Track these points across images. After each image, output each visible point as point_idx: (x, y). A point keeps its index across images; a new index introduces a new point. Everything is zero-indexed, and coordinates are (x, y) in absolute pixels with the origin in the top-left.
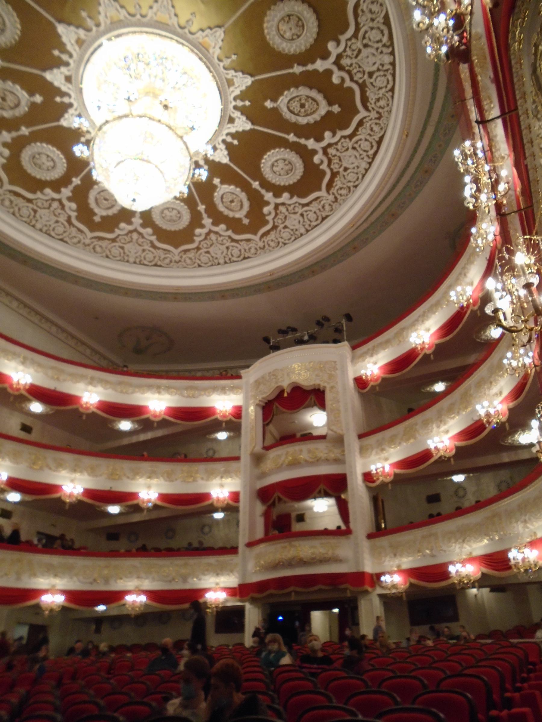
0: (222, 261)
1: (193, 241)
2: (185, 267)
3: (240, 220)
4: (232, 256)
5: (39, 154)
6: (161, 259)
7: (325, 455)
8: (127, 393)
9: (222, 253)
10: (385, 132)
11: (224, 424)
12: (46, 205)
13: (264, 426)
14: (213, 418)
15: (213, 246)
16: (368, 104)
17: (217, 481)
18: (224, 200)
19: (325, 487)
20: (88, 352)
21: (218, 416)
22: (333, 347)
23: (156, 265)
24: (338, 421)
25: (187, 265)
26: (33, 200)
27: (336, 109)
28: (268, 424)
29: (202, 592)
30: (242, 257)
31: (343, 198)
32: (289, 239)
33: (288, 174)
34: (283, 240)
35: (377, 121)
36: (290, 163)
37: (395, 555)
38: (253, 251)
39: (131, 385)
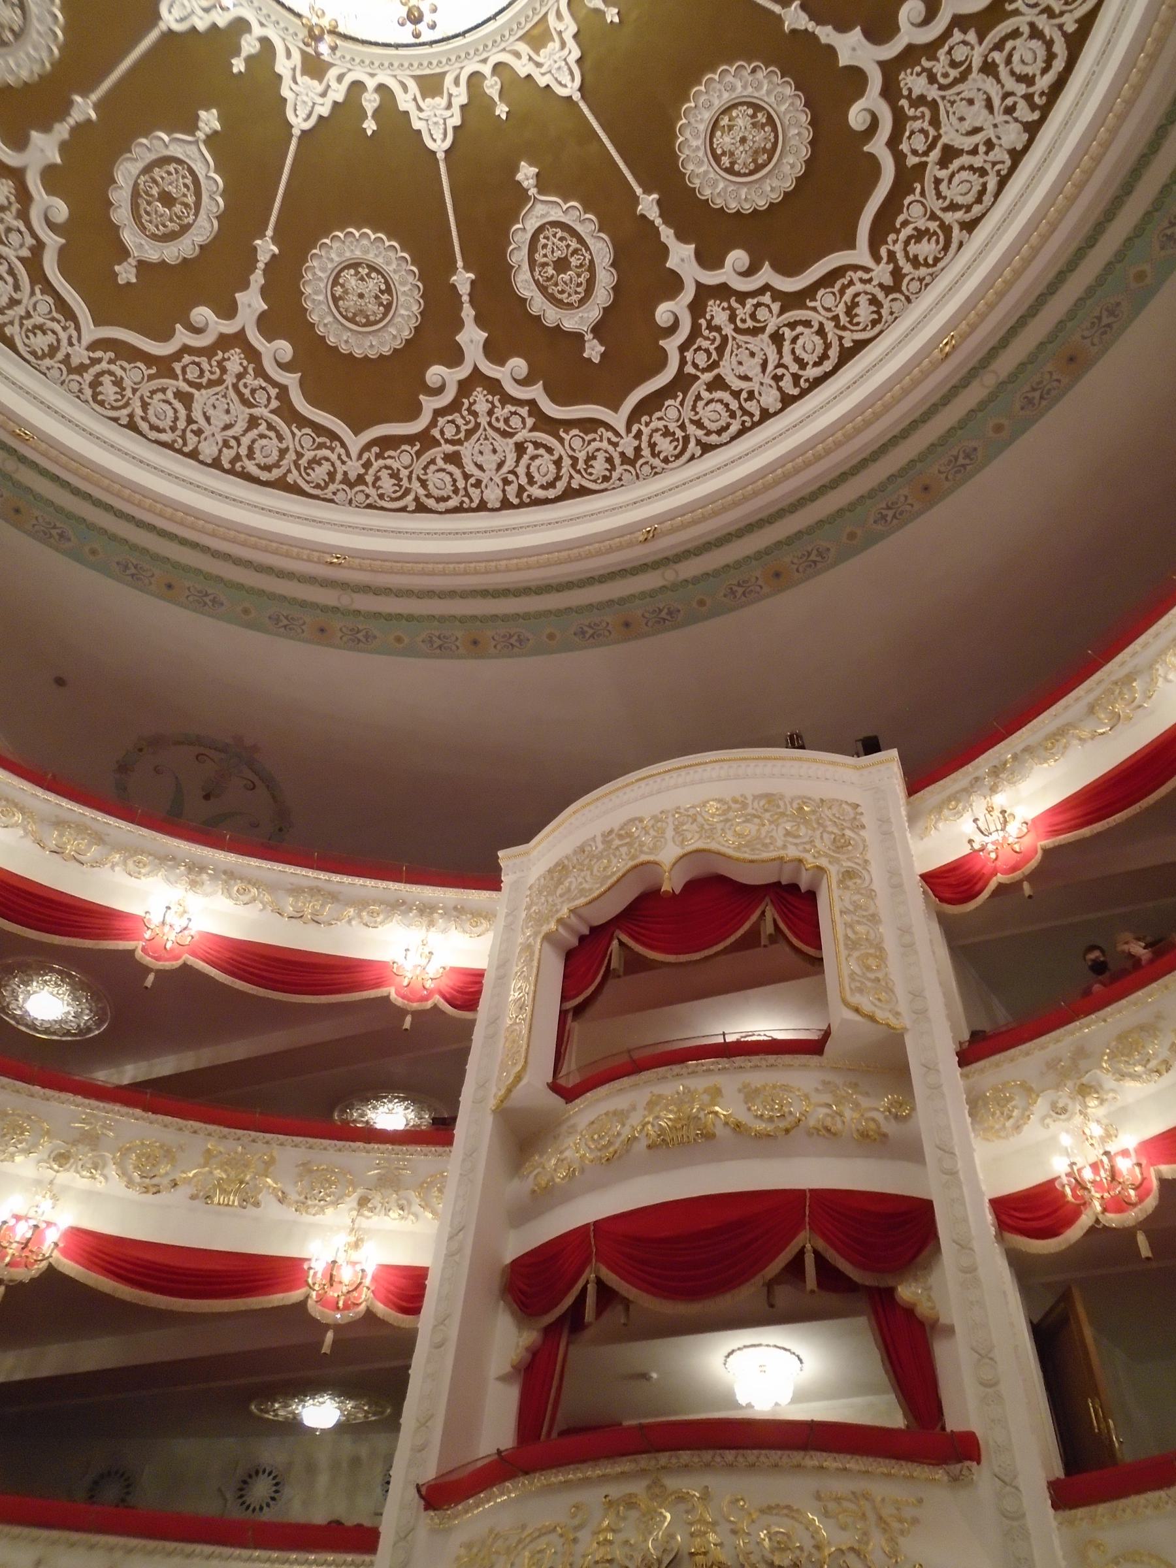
10: (28, 362)
16: (111, 355)
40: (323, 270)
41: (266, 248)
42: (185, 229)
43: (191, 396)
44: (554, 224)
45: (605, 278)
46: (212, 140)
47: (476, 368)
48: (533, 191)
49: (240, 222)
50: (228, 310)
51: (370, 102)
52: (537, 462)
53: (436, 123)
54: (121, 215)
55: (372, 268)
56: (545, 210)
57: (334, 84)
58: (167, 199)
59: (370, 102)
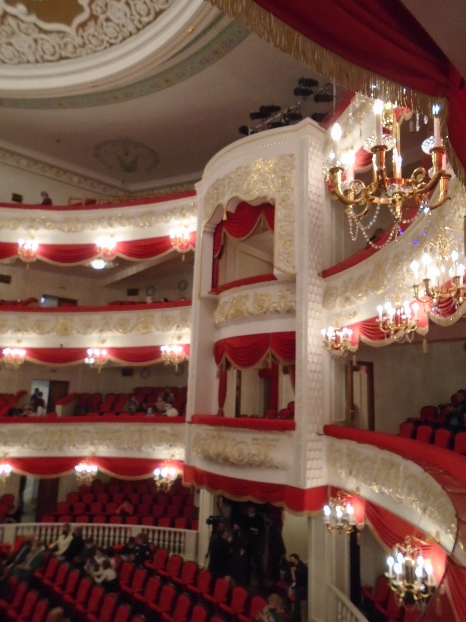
2: (95, 52)
4: (140, 15)
6: (62, 46)
7: (275, 305)
8: (76, 231)
9: (126, 14)
11: (183, 257)
13: (214, 260)
14: (170, 250)
17: (173, 332)
19: (274, 352)
20: (76, 179)
21: (176, 247)
22: (290, 131)
23: (61, 58)
24: (288, 253)
25: (96, 46)
28: (220, 256)
29: (151, 464)
30: (153, 12)
37: (350, 473)
39: (78, 220)
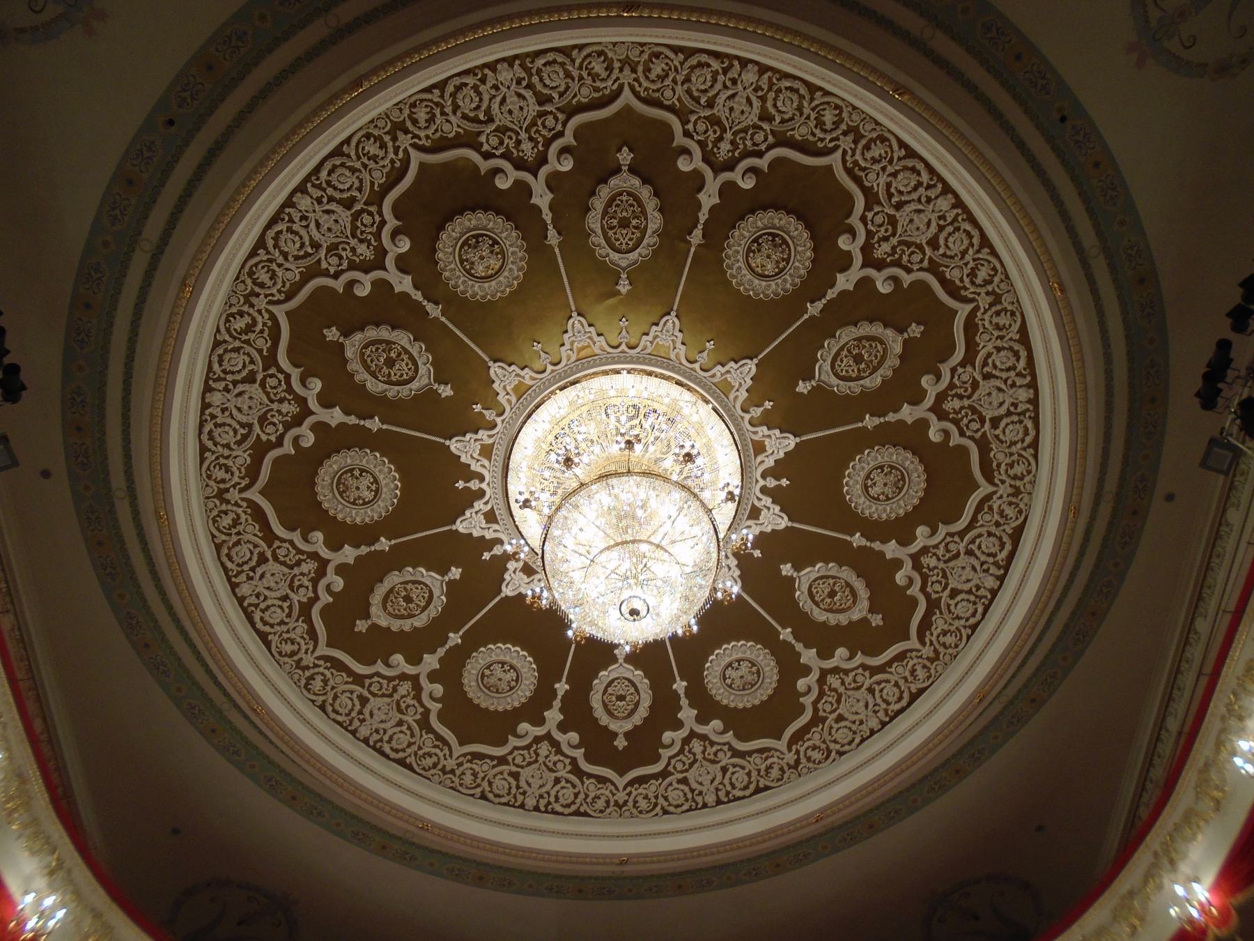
0: (530, 802)
1: (504, 742)
3: (615, 735)
5: (362, 471)
12: (293, 557)
15: (536, 765)
16: (928, 633)
18: (610, 690)
26: (278, 538)
27: (877, 620)
31: (811, 765)
32: (677, 806)
33: (744, 689)
34: (665, 804)
35: (928, 664)
36: (758, 673)
38: (600, 804)
40: (870, 507)
41: (857, 540)
42: (848, 585)
43: (952, 590)
44: (833, 367)
45: (866, 329)
46: (798, 568)
47: (930, 410)
48: (814, 383)
49: (842, 554)
50: (898, 564)
51: (771, 483)
52: (998, 364)
53: (780, 444)
54: (843, 619)
55: (868, 477)
56: (823, 370)
57: (763, 503)
58: (832, 594)
59: (771, 483)
